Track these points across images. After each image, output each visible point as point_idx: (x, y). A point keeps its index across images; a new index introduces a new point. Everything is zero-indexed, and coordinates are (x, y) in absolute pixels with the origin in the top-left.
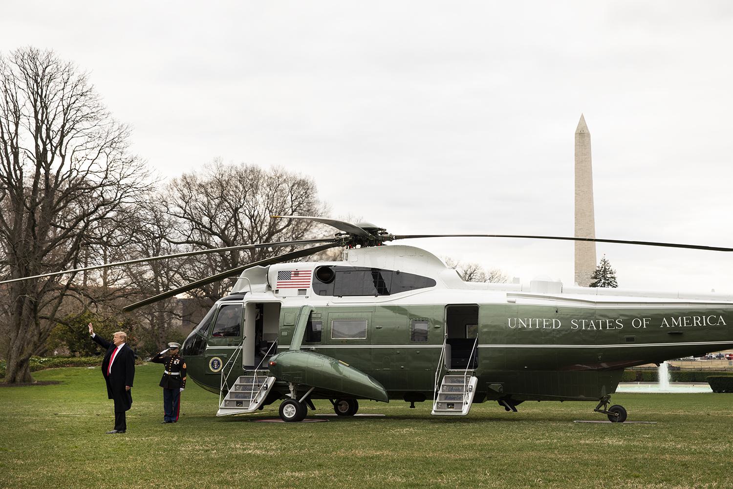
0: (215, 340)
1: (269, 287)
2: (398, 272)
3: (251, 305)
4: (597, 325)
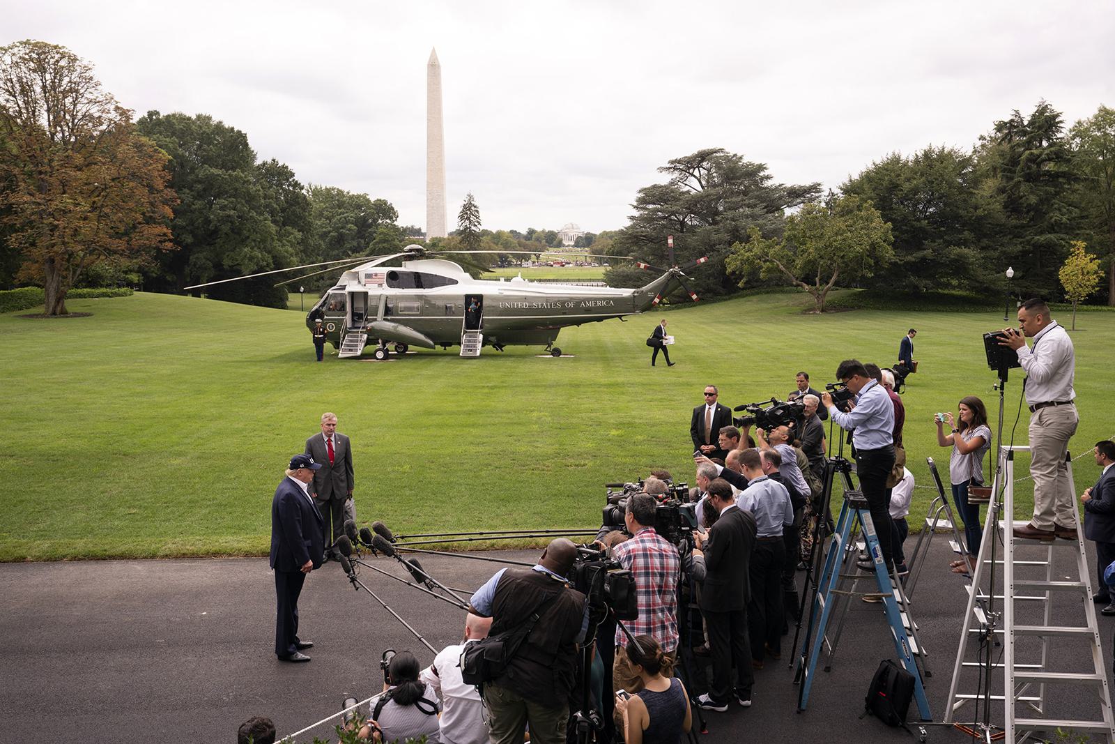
0: (330, 313)
1: (359, 282)
2: (436, 275)
3: (349, 293)
4: (547, 305)
